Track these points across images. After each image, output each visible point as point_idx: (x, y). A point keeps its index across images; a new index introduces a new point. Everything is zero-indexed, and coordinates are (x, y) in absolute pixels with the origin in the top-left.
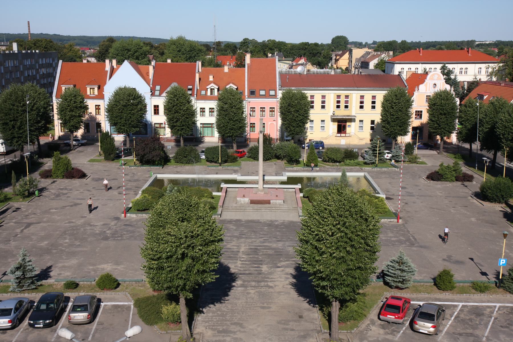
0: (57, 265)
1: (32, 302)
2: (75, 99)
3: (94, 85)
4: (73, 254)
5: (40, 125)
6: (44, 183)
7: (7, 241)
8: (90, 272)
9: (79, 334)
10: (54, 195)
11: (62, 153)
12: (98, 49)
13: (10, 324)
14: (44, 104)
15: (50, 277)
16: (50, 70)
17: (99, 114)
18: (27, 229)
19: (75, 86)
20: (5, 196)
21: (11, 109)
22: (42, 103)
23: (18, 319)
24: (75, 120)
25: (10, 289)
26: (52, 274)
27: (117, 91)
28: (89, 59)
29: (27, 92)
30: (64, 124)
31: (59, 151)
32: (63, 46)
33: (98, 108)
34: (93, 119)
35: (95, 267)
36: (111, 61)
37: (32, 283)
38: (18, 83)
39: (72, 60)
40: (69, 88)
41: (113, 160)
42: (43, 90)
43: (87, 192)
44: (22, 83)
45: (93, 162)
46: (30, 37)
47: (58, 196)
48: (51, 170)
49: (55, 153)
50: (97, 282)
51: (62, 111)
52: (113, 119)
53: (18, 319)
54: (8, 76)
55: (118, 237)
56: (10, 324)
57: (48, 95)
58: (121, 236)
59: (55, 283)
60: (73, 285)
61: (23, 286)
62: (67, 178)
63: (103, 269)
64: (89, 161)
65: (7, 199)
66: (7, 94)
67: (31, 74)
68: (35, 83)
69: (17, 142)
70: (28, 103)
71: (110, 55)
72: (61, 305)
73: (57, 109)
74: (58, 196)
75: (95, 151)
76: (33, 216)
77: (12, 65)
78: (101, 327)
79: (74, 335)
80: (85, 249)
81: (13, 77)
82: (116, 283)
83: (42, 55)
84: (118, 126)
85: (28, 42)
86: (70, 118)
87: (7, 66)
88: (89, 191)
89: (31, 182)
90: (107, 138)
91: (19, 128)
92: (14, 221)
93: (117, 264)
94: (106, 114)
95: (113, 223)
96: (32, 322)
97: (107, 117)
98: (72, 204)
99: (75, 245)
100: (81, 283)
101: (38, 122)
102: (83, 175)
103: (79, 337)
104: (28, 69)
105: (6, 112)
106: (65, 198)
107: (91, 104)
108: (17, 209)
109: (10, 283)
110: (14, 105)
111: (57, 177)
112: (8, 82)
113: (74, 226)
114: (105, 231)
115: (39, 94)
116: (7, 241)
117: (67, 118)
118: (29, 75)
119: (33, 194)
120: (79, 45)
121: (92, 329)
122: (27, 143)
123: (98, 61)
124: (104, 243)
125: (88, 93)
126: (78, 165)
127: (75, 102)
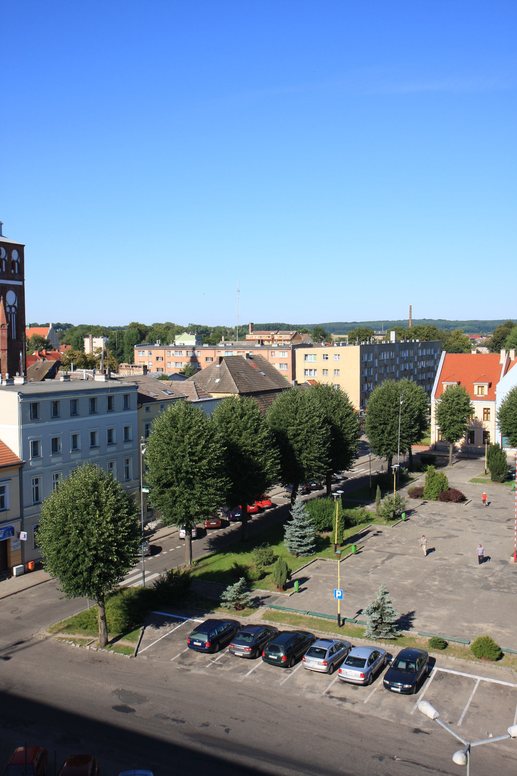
0: (422, 613)
1: (389, 656)
2: (459, 399)
3: (483, 382)
4: (442, 602)
5: (413, 430)
6: (413, 504)
7: (365, 572)
9: (445, 713)
10: (424, 521)
11: (436, 468)
12: (492, 336)
13: (363, 679)
14: (420, 405)
15: (412, 626)
16: (431, 363)
17: (487, 420)
18: (389, 561)
19: (459, 383)
20: (367, 516)
21: (382, 410)
22: (418, 403)
23: (372, 674)
24: (456, 427)
25: (366, 634)
26: (414, 623)
27: (513, 390)
28: (480, 349)
29: (401, 390)
30: (443, 430)
31: (434, 465)
32: (448, 333)
33: (486, 411)
34: (478, 425)
35: (470, 625)
36: (507, 352)
37: (391, 631)
38: (392, 378)
39: (458, 351)
40: (451, 386)
41: (503, 482)
42: (420, 387)
43: (466, 521)
44: (397, 379)
45: (476, 482)
46: (410, 325)
47: (429, 522)
48: (423, 488)
49: (429, 467)
50: (472, 646)
51: (441, 414)
52: (506, 427)
53: (372, 674)
54: (382, 371)
55: (504, 588)
56: (363, 679)
57: (426, 394)
58: (509, 587)
59: (417, 637)
60: (441, 645)
61: (380, 632)
62: (442, 500)
63: (481, 630)
64: (471, 481)
65: (368, 520)
66: (379, 391)
67: (408, 368)
68: (411, 380)
69: (385, 450)
70: (401, 403)
71: (508, 343)
72: (425, 667)
73: (435, 411)
74: (429, 522)
75: (479, 469)
76: (397, 545)
77: (388, 358)
78: (475, 710)
79: (438, 715)
80: (458, 598)
81: (388, 371)
82: (498, 653)
83: (425, 346)
84: (512, 437)
85: (408, 330)
86: (450, 423)
87: (382, 358)
88: (468, 520)
89: (398, 501)
90: (496, 451)
91: (390, 434)
92: (375, 548)
93: (501, 625)
94: (497, 420)
95: (498, 568)
96: (388, 682)
97: (499, 425)
98: (445, 535)
99: (446, 590)
100: (451, 643)
101: (412, 427)
102: (462, 499)
103: (445, 718)
104: (406, 362)
105: (376, 413)
106: (438, 526)
107: (478, 407)
108: (378, 532)
109: (365, 627)
110: (385, 406)
111: (430, 498)
112: (382, 378)
113: (446, 565)
114: (486, 578)
115: (416, 392)
116: (365, 572)
117: (447, 423)
118: (405, 370)
119: (399, 516)
120: (468, 332)
121: (462, 710)
122: (397, 452)
123: (492, 351)
124: (484, 594)
125: (476, 393)
126: (457, 485)
127: (458, 403)
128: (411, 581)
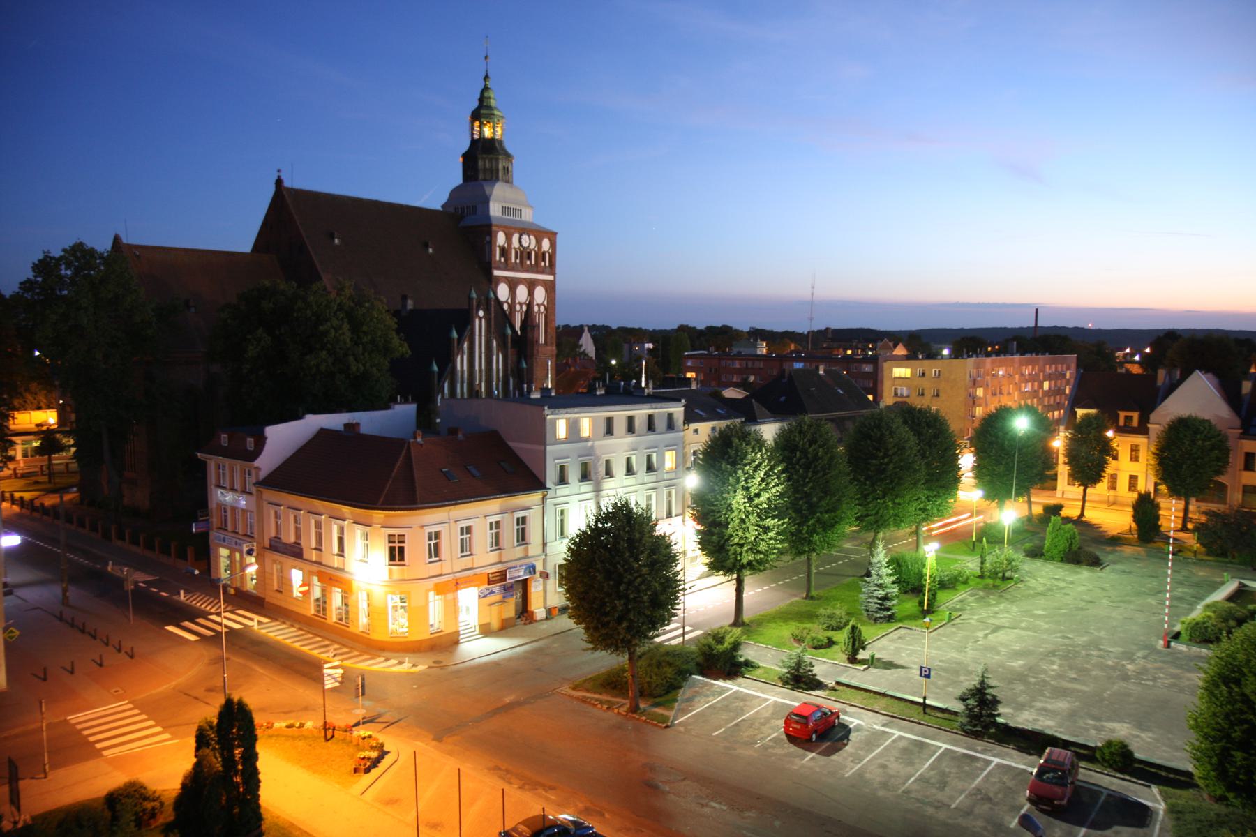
8: (1087, 730)
35: (1098, 724)
58: (1155, 679)
63: (1113, 731)
80: (1084, 688)
93: (1141, 725)
128: (1021, 662)
